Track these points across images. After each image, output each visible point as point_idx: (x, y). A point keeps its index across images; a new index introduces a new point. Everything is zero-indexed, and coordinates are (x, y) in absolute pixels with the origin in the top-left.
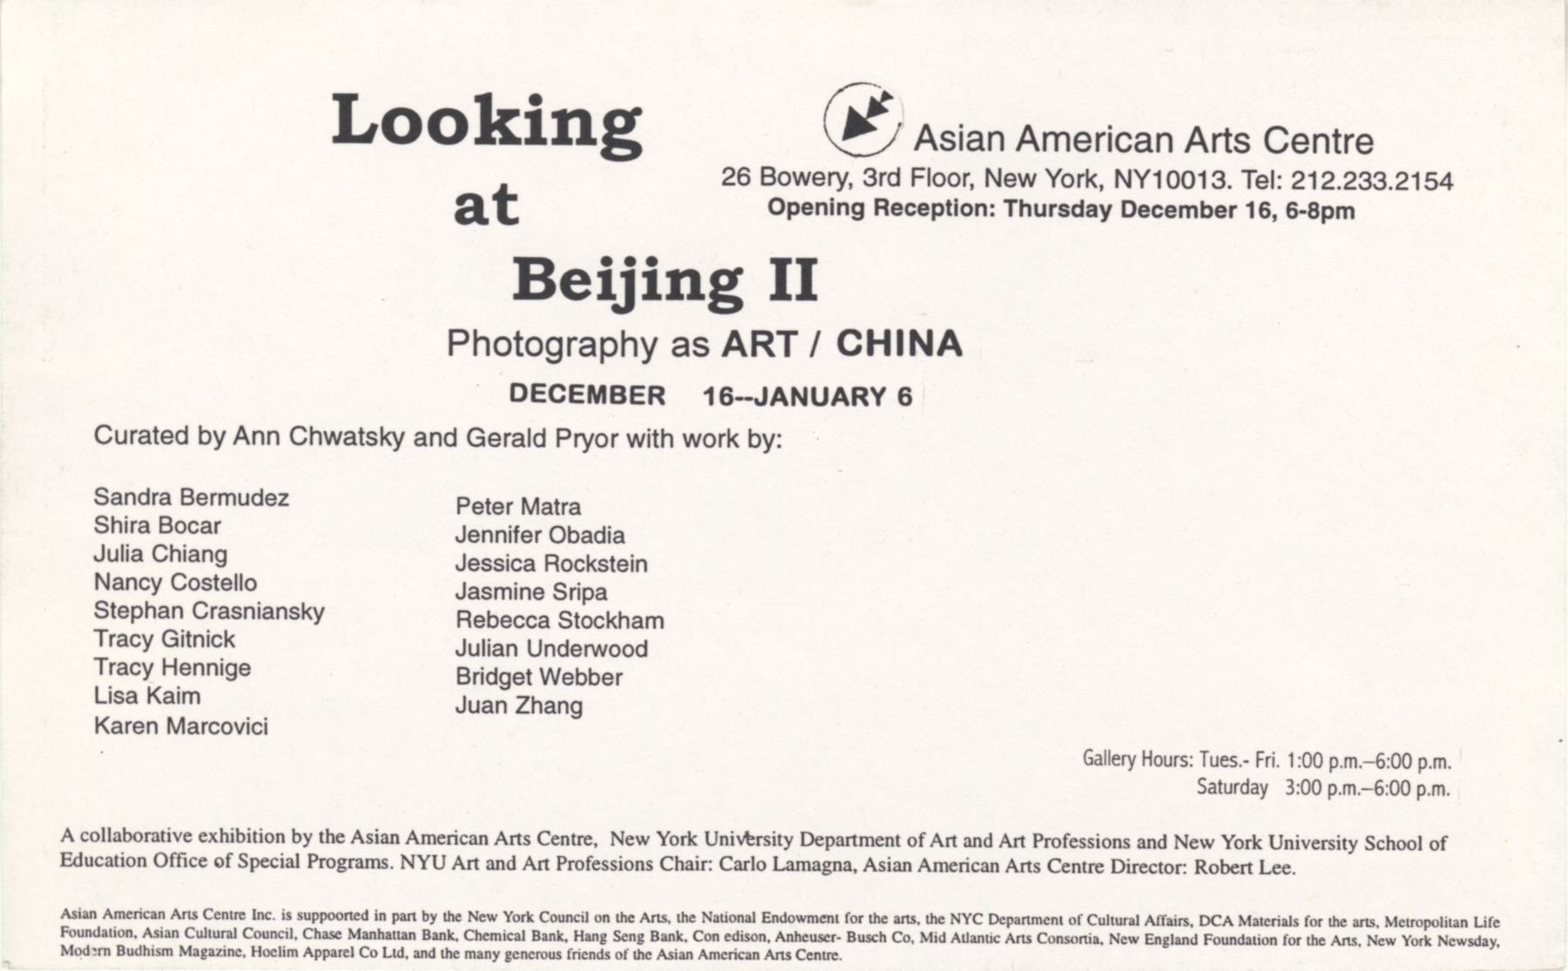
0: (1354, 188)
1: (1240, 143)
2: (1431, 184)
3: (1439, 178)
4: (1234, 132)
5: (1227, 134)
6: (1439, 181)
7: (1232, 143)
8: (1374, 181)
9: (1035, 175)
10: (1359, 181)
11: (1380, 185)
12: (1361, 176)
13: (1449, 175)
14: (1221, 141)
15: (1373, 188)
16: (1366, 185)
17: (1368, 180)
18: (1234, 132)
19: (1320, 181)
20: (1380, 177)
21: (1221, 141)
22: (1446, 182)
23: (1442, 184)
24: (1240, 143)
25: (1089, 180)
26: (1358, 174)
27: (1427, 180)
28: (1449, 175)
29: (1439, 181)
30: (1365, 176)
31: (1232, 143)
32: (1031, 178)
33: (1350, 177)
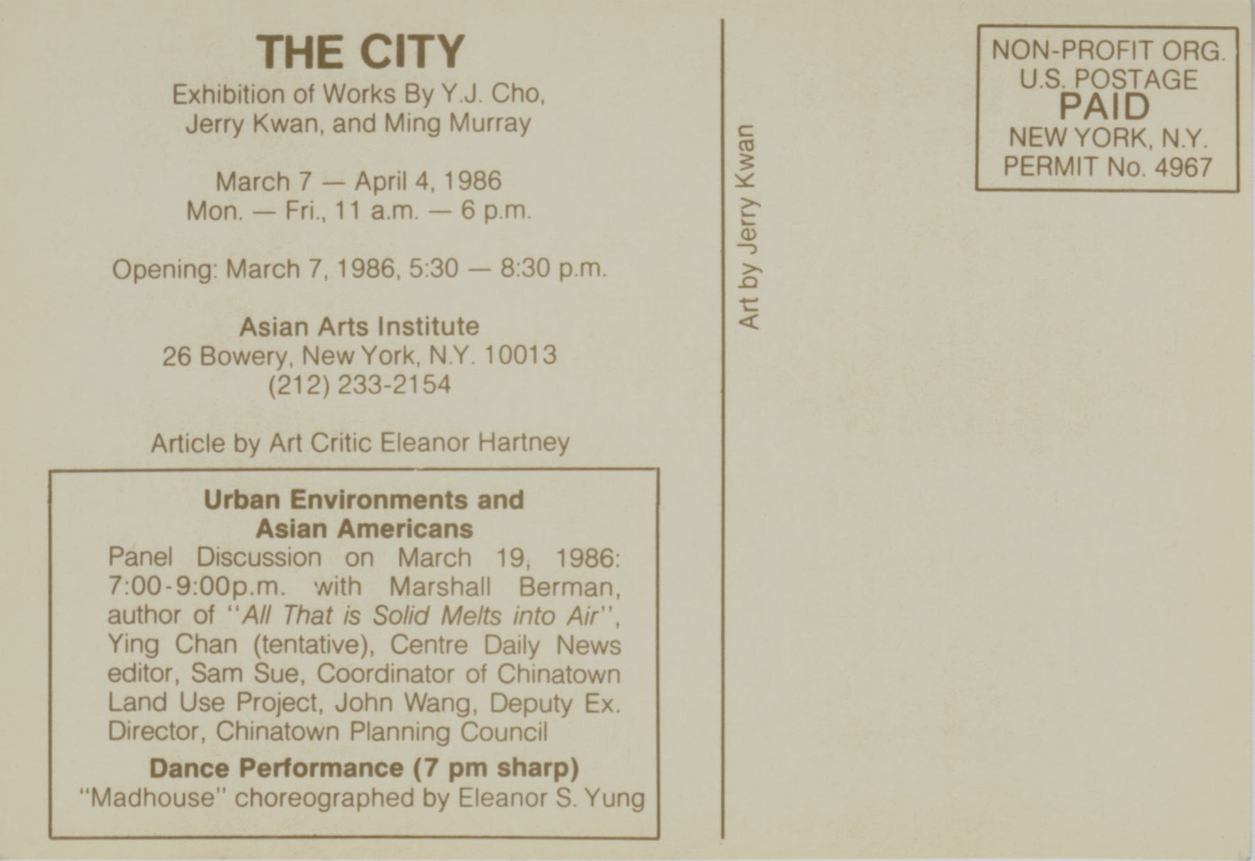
0: (349, 393)
1: (363, 329)
2: (429, 387)
3: (437, 380)
4: (356, 321)
5: (351, 323)
6: (437, 383)
7: (355, 329)
8: (369, 384)
9: (353, 353)
10: (355, 384)
11: (375, 388)
12: (356, 379)
13: (446, 378)
14: (346, 328)
15: (367, 392)
16: (360, 388)
17: (362, 384)
18: (356, 321)
19: (306, 385)
20: (375, 380)
21: (346, 328)
22: (444, 384)
23: (440, 387)
24: (363, 329)
25: (407, 357)
26: (352, 377)
27: (426, 382)
28: (446, 378)
29: (437, 383)
30: (360, 380)
31: (355, 329)
32: (349, 355)
33: (345, 380)
